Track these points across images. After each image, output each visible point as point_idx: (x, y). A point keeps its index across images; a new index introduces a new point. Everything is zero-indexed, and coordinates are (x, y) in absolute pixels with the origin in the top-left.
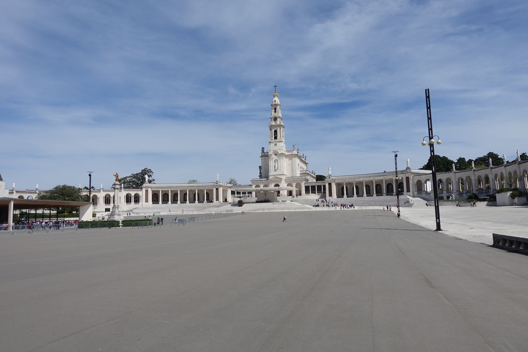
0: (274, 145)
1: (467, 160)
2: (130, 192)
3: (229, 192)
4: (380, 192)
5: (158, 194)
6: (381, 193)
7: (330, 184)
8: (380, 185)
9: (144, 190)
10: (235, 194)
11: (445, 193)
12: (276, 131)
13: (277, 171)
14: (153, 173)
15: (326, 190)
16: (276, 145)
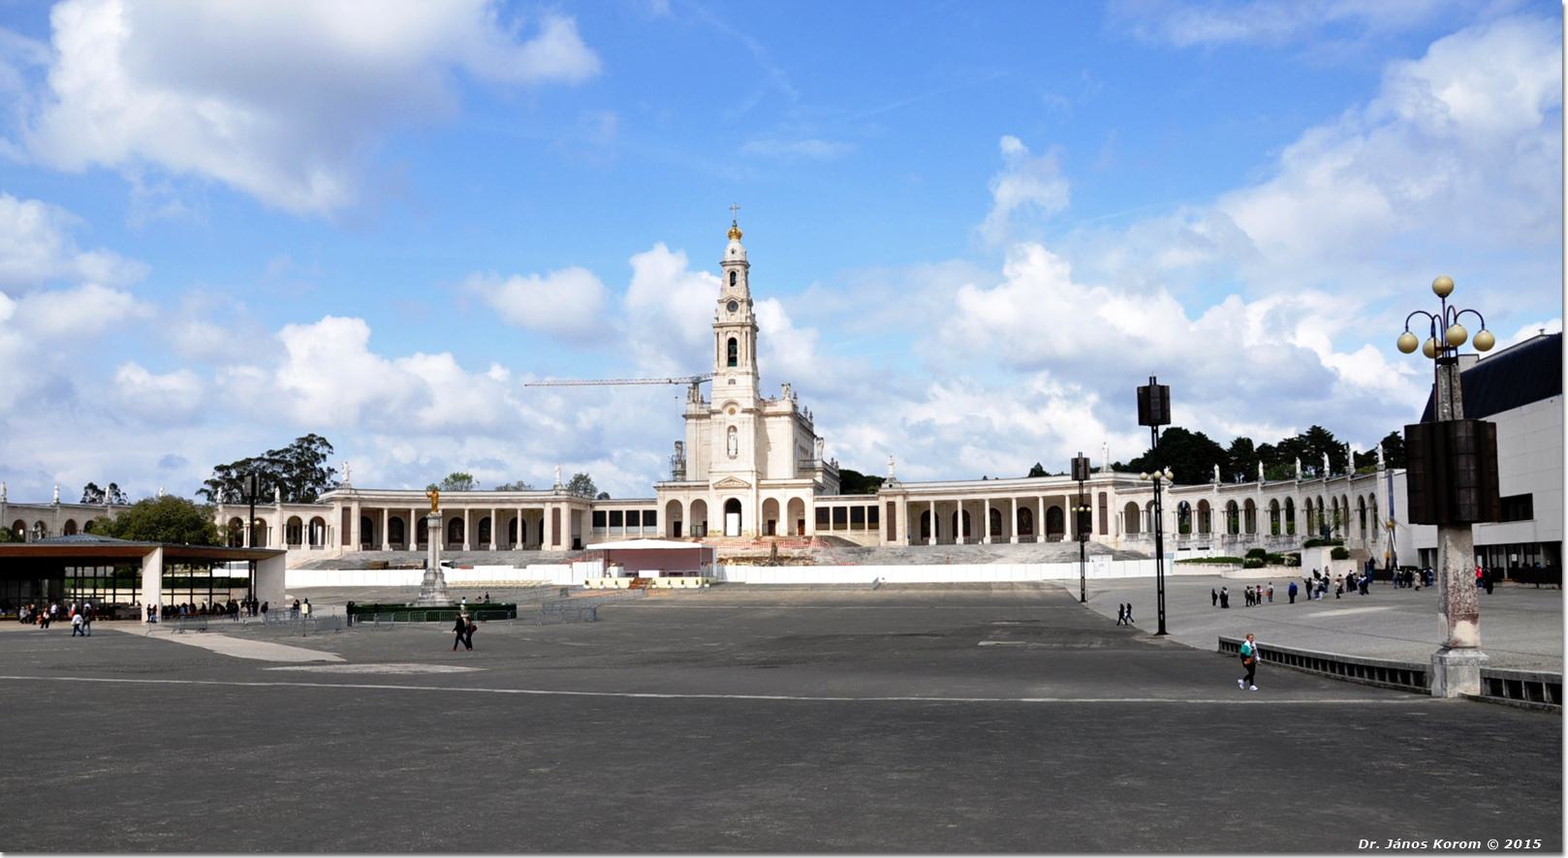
0: (727, 381)
1: (1256, 445)
2: (300, 514)
3: (588, 518)
4: (1028, 529)
5: (373, 520)
6: (1031, 532)
7: (891, 506)
8: (1029, 512)
9: (338, 508)
10: (605, 525)
11: (1194, 541)
12: (732, 342)
13: (735, 460)
14: (331, 447)
15: (880, 521)
16: (732, 382)
